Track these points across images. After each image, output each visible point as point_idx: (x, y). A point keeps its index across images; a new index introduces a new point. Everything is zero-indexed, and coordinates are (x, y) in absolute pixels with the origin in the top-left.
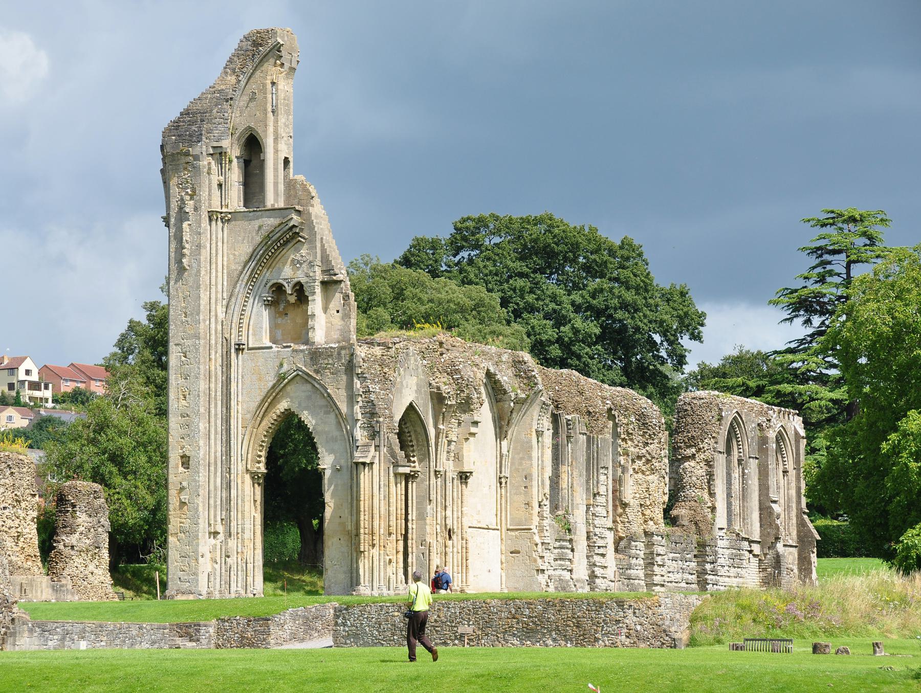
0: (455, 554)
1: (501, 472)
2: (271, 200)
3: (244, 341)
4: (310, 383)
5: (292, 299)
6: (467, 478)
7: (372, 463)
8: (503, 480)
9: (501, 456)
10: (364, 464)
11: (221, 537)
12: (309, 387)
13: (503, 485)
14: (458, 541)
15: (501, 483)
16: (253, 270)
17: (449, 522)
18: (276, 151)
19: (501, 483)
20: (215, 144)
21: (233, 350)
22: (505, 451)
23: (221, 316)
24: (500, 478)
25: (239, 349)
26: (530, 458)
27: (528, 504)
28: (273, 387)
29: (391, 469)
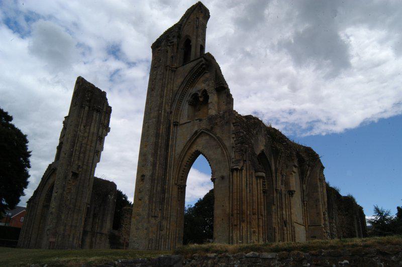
0: (288, 234)
1: (304, 199)
2: (192, 57)
3: (178, 121)
4: (209, 134)
5: (201, 99)
6: (292, 194)
7: (242, 169)
8: (305, 202)
9: (303, 191)
10: (237, 170)
11: (158, 219)
12: (208, 137)
13: (305, 205)
14: (289, 227)
15: (304, 204)
16: (184, 88)
17: (284, 217)
18: (197, 41)
19: (304, 204)
20: (171, 41)
21: (172, 125)
22: (305, 188)
23: (168, 110)
24: (304, 201)
25: (176, 124)
26: (317, 192)
27: (318, 213)
28: (190, 140)
29: (254, 173)
